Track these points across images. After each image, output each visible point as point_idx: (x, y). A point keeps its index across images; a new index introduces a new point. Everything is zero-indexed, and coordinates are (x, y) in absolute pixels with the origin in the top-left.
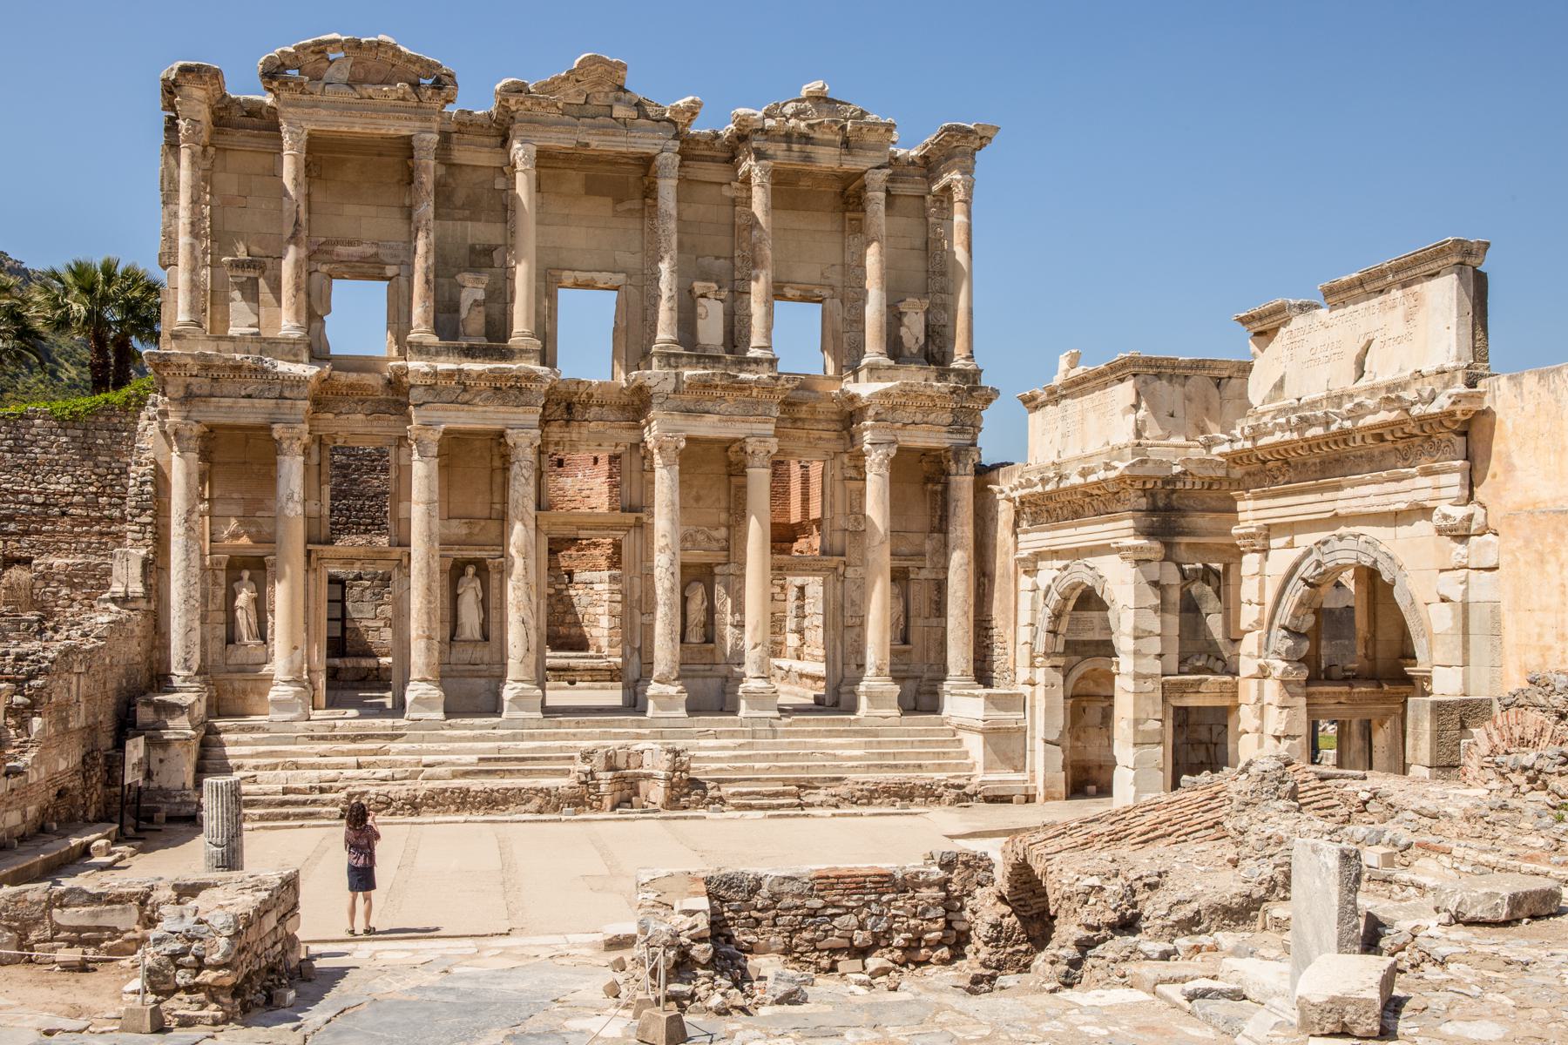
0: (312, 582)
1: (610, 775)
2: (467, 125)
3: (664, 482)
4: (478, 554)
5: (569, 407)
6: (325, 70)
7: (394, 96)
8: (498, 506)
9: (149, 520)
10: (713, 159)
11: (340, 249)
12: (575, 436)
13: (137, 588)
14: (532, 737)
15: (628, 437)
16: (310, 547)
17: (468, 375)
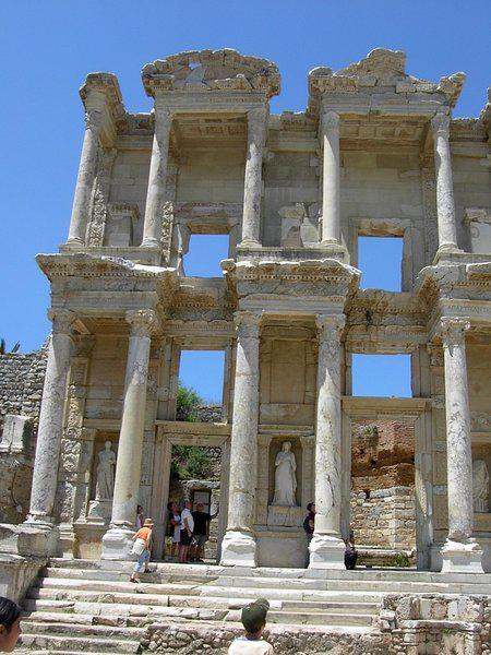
0: (158, 453)
1: (415, 623)
2: (289, 124)
3: (454, 363)
4: (292, 433)
5: (368, 315)
6: (186, 75)
7: (234, 85)
8: (310, 394)
9: (37, 397)
10: (471, 140)
11: (196, 208)
12: (374, 339)
13: (18, 446)
14: (335, 588)
15: (419, 339)
16: (158, 422)
17: (284, 272)
